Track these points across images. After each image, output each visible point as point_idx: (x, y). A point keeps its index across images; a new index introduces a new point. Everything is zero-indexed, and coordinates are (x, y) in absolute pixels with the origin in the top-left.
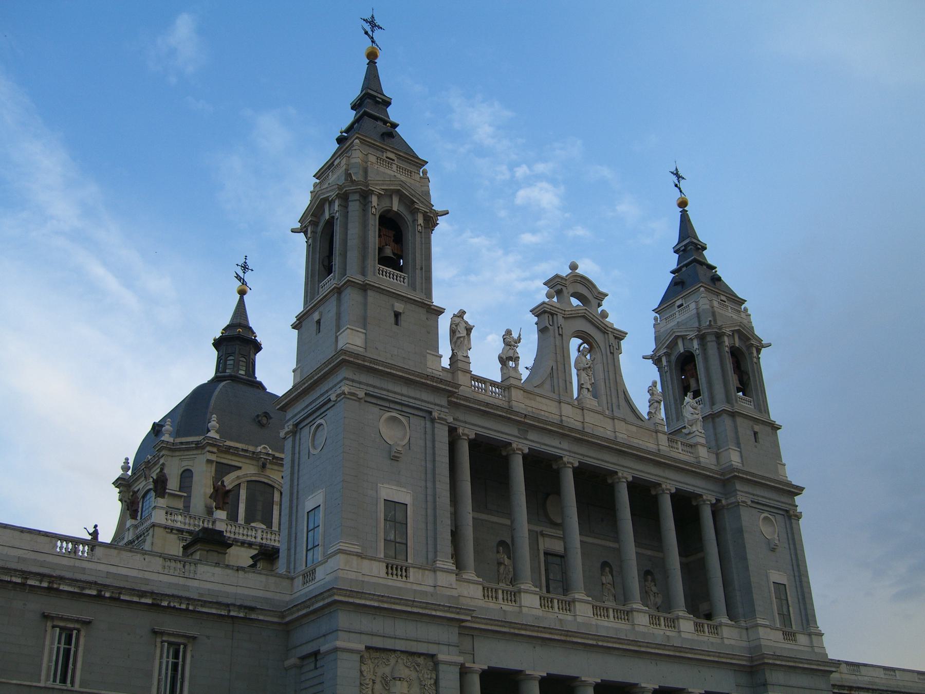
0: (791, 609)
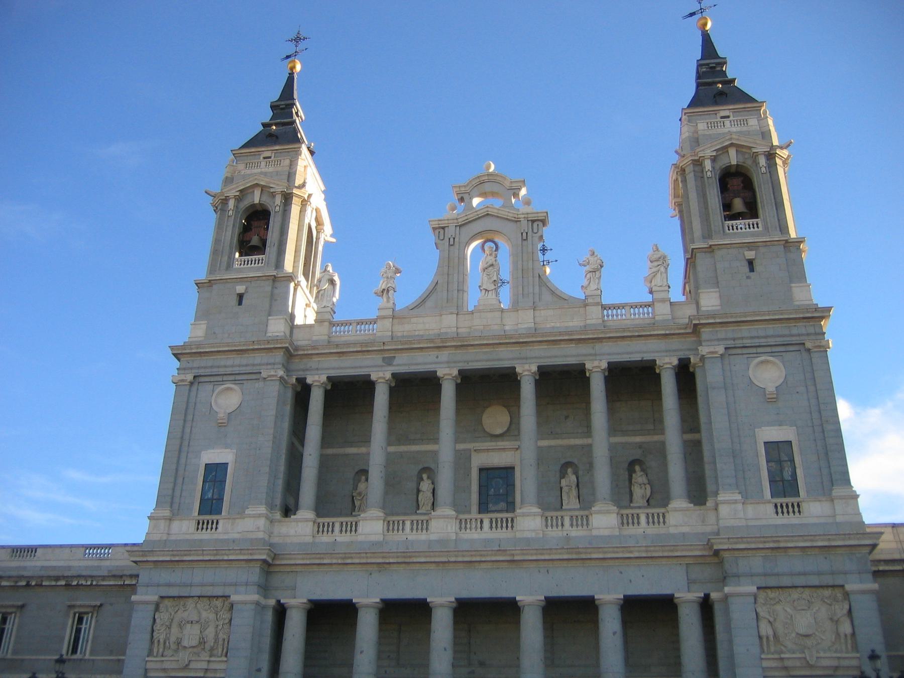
0: (799, 472)
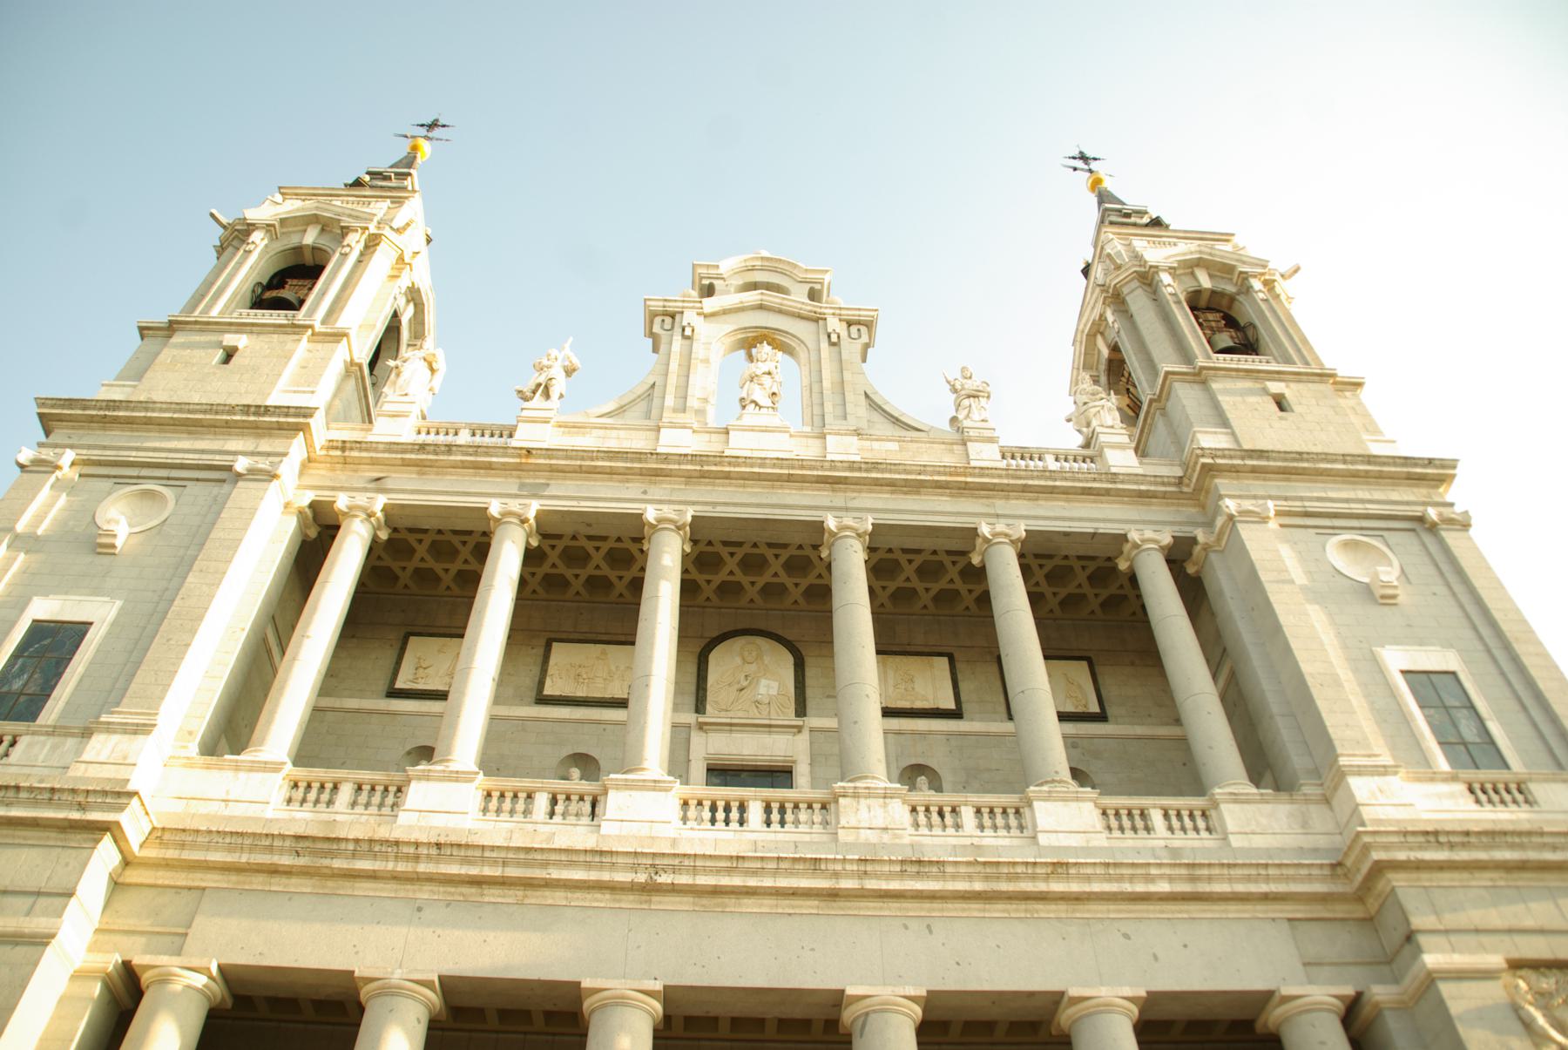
0: (1494, 727)
